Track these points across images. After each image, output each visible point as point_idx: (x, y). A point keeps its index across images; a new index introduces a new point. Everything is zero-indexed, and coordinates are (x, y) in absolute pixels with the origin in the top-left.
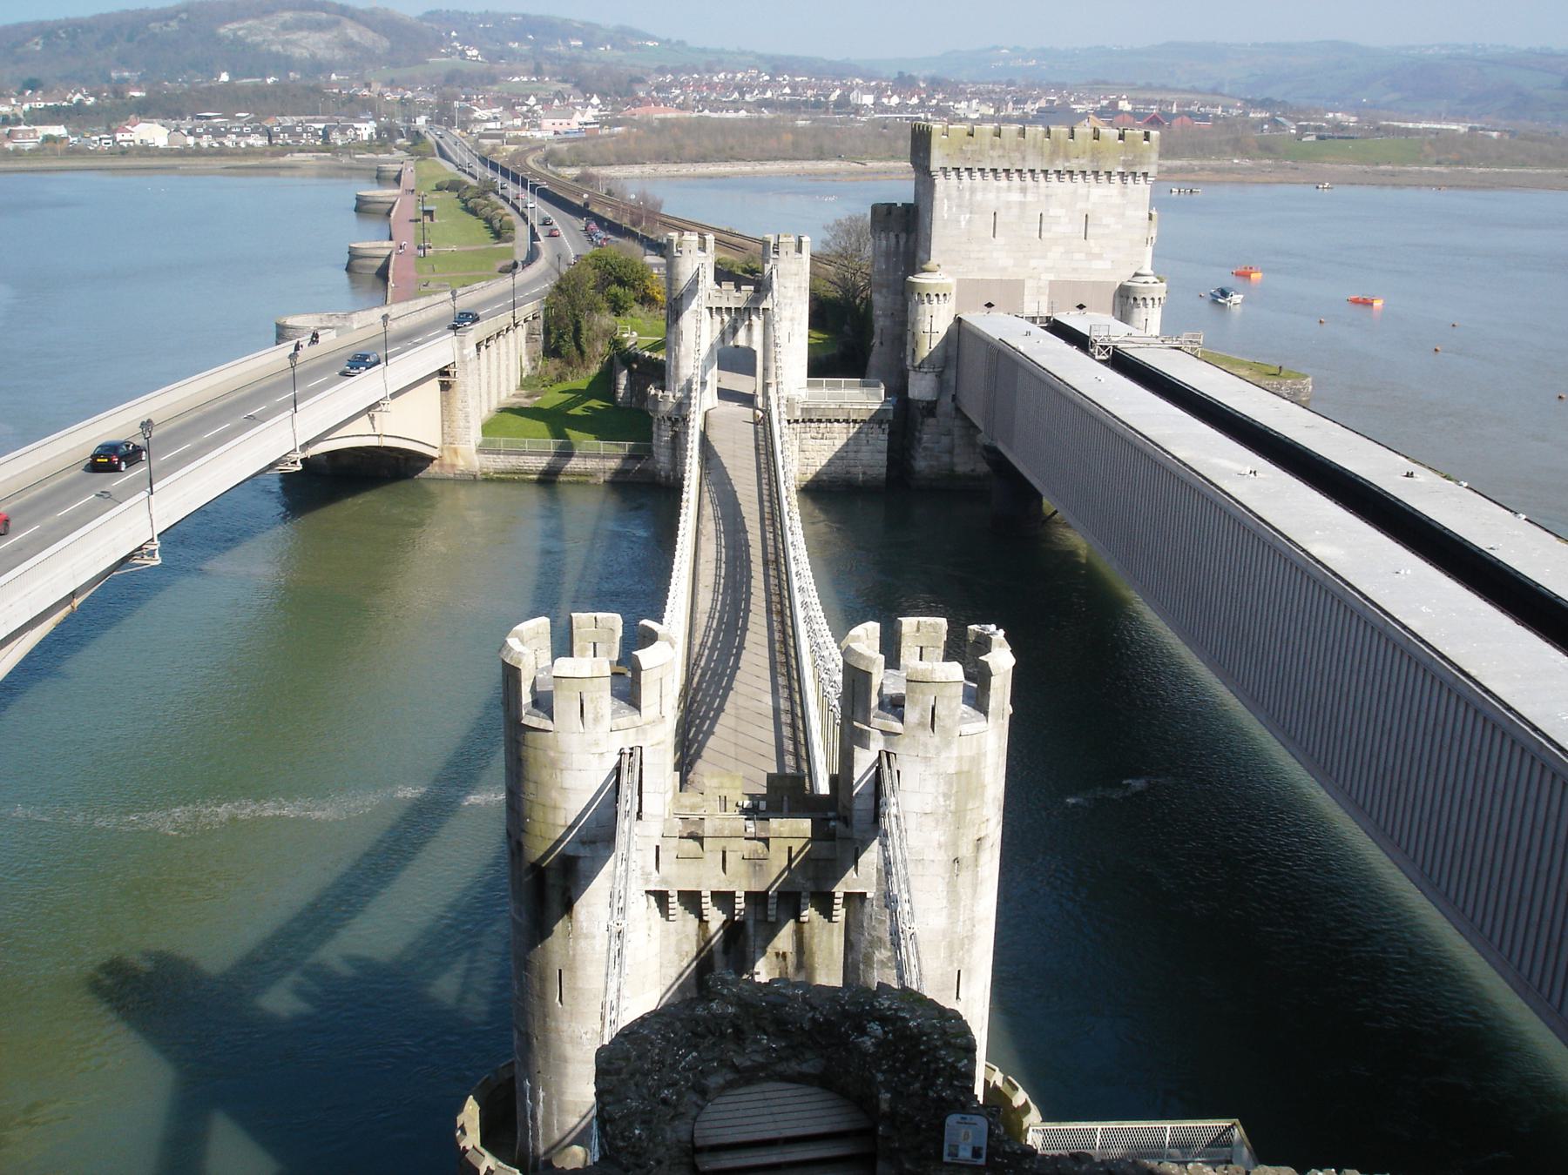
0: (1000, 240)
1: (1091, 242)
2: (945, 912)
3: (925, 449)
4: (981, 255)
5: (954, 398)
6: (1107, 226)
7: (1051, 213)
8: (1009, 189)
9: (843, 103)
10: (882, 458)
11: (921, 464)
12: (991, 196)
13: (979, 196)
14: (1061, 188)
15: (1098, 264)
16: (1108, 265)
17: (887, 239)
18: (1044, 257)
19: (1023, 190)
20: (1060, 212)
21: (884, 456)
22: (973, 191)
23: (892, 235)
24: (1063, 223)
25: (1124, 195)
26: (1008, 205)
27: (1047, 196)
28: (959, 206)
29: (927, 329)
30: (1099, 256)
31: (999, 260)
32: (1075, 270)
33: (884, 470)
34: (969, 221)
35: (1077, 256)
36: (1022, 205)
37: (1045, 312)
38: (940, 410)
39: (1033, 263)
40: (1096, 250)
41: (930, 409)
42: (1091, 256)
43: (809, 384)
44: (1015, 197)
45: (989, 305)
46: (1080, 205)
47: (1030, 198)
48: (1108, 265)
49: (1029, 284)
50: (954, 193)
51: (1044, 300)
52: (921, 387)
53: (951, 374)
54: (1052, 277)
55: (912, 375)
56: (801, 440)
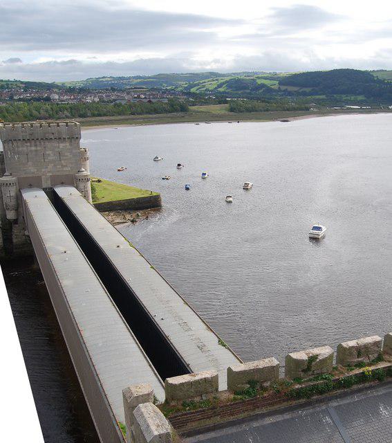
0: (30, 163)
1: (63, 162)
7: (47, 153)
8: (31, 146)
9: (48, 99)
12: (25, 149)
13: (20, 149)
14: (48, 144)
19: (36, 146)
20: (50, 152)
22: (18, 147)
24: (51, 155)
25: (71, 145)
26: (31, 151)
27: (45, 147)
30: (66, 166)
31: (32, 170)
32: (58, 171)
34: (19, 158)
36: (36, 151)
37: (50, 186)
39: (43, 170)
40: (65, 164)
41: (16, 221)
44: (33, 148)
45: (31, 185)
47: (38, 148)
51: (49, 182)
52: (11, 215)
53: (20, 210)
55: (7, 211)
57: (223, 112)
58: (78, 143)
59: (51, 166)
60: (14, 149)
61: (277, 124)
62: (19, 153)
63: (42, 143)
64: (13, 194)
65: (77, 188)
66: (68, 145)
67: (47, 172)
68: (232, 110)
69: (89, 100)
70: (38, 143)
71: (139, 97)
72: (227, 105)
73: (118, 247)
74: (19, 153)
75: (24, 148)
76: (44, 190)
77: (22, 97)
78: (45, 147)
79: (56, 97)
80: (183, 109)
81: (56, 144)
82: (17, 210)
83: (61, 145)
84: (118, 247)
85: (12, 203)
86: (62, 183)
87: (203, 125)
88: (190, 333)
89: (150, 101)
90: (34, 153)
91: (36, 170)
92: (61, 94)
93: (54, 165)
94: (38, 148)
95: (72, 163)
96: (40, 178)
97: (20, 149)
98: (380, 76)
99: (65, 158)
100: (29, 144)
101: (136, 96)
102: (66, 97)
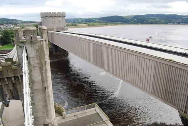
0: (51, 24)
2: (41, 76)
13: (48, 19)
20: (56, 21)
24: (57, 22)
30: (61, 25)
31: (51, 26)
44: (52, 19)
47: (53, 19)
48: (62, 26)
61: (101, 27)
67: (55, 27)
68: (88, 25)
74: (48, 21)
75: (49, 19)
80: (75, 25)
81: (58, 18)
83: (60, 19)
87: (81, 28)
94: (53, 19)
97: (48, 19)
98: (124, 17)
100: (50, 18)
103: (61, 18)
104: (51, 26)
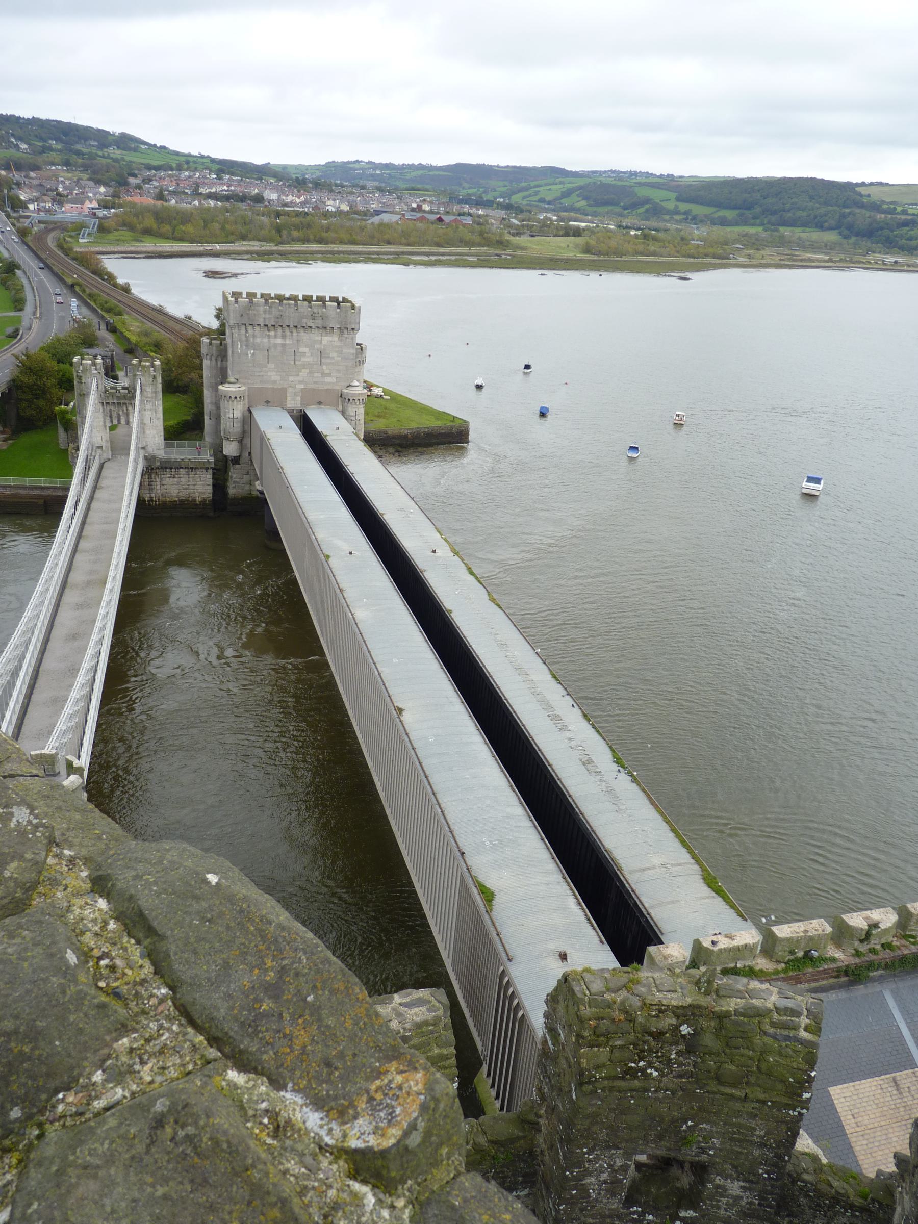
0: (271, 366)
1: (324, 367)
3: (234, 482)
4: (262, 374)
5: (250, 454)
6: (333, 358)
7: (301, 350)
8: (276, 336)
9: (259, 199)
10: (210, 489)
11: (232, 491)
13: (258, 340)
14: (304, 336)
15: (328, 380)
16: (334, 380)
17: (211, 359)
18: (298, 375)
19: (284, 337)
20: (306, 350)
21: (211, 487)
22: (254, 336)
23: (213, 358)
25: (341, 341)
26: (276, 345)
27: (298, 341)
28: (247, 346)
29: (231, 416)
30: (329, 375)
31: (272, 376)
32: (315, 383)
33: (211, 495)
34: (253, 355)
35: (316, 375)
36: (284, 345)
38: (242, 461)
39: (291, 379)
40: (327, 371)
41: (236, 460)
42: (324, 375)
43: (167, 446)
44: (279, 341)
45: (268, 402)
46: (317, 346)
47: (288, 342)
48: (334, 380)
49: (290, 390)
50: (244, 338)
52: (230, 449)
53: (247, 441)
54: (302, 386)
55: (225, 442)
56: (161, 479)
57: (570, 254)
58: (353, 339)
59: (304, 373)
60: (247, 340)
62: (255, 347)
63: (295, 334)
64: (238, 414)
65: (343, 413)
66: (336, 338)
68: (587, 250)
69: (331, 205)
70: (288, 333)
71: (419, 207)
72: (579, 240)
73: (434, 551)
74: (255, 347)
76: (290, 412)
77: (213, 190)
78: (298, 341)
79: (274, 196)
81: (315, 336)
82: (241, 441)
83: (326, 339)
84: (434, 551)
85: (237, 429)
86: (320, 403)
88: (568, 734)
89: (440, 220)
90: (279, 349)
91: (278, 378)
92: (283, 193)
93: (311, 372)
94: (288, 342)
95: (338, 371)
96: (284, 391)
97: (258, 340)
99: (329, 361)
100: (272, 333)
101: (414, 205)
102: (290, 198)
103: (334, 338)
104: (274, 376)
